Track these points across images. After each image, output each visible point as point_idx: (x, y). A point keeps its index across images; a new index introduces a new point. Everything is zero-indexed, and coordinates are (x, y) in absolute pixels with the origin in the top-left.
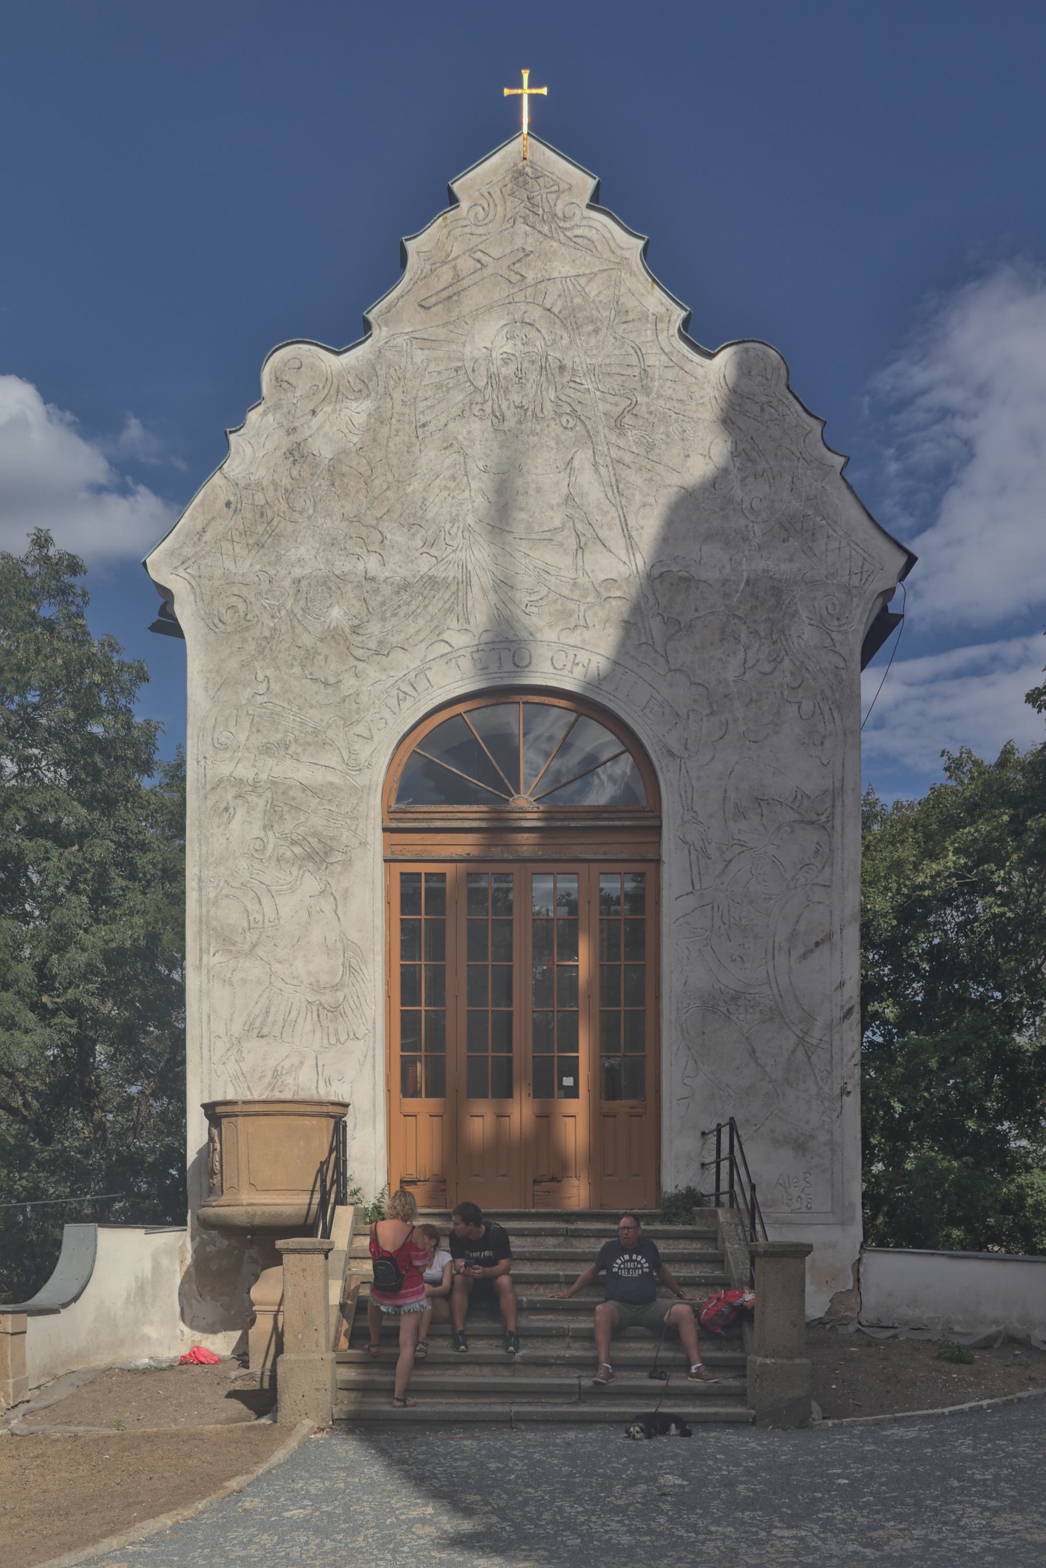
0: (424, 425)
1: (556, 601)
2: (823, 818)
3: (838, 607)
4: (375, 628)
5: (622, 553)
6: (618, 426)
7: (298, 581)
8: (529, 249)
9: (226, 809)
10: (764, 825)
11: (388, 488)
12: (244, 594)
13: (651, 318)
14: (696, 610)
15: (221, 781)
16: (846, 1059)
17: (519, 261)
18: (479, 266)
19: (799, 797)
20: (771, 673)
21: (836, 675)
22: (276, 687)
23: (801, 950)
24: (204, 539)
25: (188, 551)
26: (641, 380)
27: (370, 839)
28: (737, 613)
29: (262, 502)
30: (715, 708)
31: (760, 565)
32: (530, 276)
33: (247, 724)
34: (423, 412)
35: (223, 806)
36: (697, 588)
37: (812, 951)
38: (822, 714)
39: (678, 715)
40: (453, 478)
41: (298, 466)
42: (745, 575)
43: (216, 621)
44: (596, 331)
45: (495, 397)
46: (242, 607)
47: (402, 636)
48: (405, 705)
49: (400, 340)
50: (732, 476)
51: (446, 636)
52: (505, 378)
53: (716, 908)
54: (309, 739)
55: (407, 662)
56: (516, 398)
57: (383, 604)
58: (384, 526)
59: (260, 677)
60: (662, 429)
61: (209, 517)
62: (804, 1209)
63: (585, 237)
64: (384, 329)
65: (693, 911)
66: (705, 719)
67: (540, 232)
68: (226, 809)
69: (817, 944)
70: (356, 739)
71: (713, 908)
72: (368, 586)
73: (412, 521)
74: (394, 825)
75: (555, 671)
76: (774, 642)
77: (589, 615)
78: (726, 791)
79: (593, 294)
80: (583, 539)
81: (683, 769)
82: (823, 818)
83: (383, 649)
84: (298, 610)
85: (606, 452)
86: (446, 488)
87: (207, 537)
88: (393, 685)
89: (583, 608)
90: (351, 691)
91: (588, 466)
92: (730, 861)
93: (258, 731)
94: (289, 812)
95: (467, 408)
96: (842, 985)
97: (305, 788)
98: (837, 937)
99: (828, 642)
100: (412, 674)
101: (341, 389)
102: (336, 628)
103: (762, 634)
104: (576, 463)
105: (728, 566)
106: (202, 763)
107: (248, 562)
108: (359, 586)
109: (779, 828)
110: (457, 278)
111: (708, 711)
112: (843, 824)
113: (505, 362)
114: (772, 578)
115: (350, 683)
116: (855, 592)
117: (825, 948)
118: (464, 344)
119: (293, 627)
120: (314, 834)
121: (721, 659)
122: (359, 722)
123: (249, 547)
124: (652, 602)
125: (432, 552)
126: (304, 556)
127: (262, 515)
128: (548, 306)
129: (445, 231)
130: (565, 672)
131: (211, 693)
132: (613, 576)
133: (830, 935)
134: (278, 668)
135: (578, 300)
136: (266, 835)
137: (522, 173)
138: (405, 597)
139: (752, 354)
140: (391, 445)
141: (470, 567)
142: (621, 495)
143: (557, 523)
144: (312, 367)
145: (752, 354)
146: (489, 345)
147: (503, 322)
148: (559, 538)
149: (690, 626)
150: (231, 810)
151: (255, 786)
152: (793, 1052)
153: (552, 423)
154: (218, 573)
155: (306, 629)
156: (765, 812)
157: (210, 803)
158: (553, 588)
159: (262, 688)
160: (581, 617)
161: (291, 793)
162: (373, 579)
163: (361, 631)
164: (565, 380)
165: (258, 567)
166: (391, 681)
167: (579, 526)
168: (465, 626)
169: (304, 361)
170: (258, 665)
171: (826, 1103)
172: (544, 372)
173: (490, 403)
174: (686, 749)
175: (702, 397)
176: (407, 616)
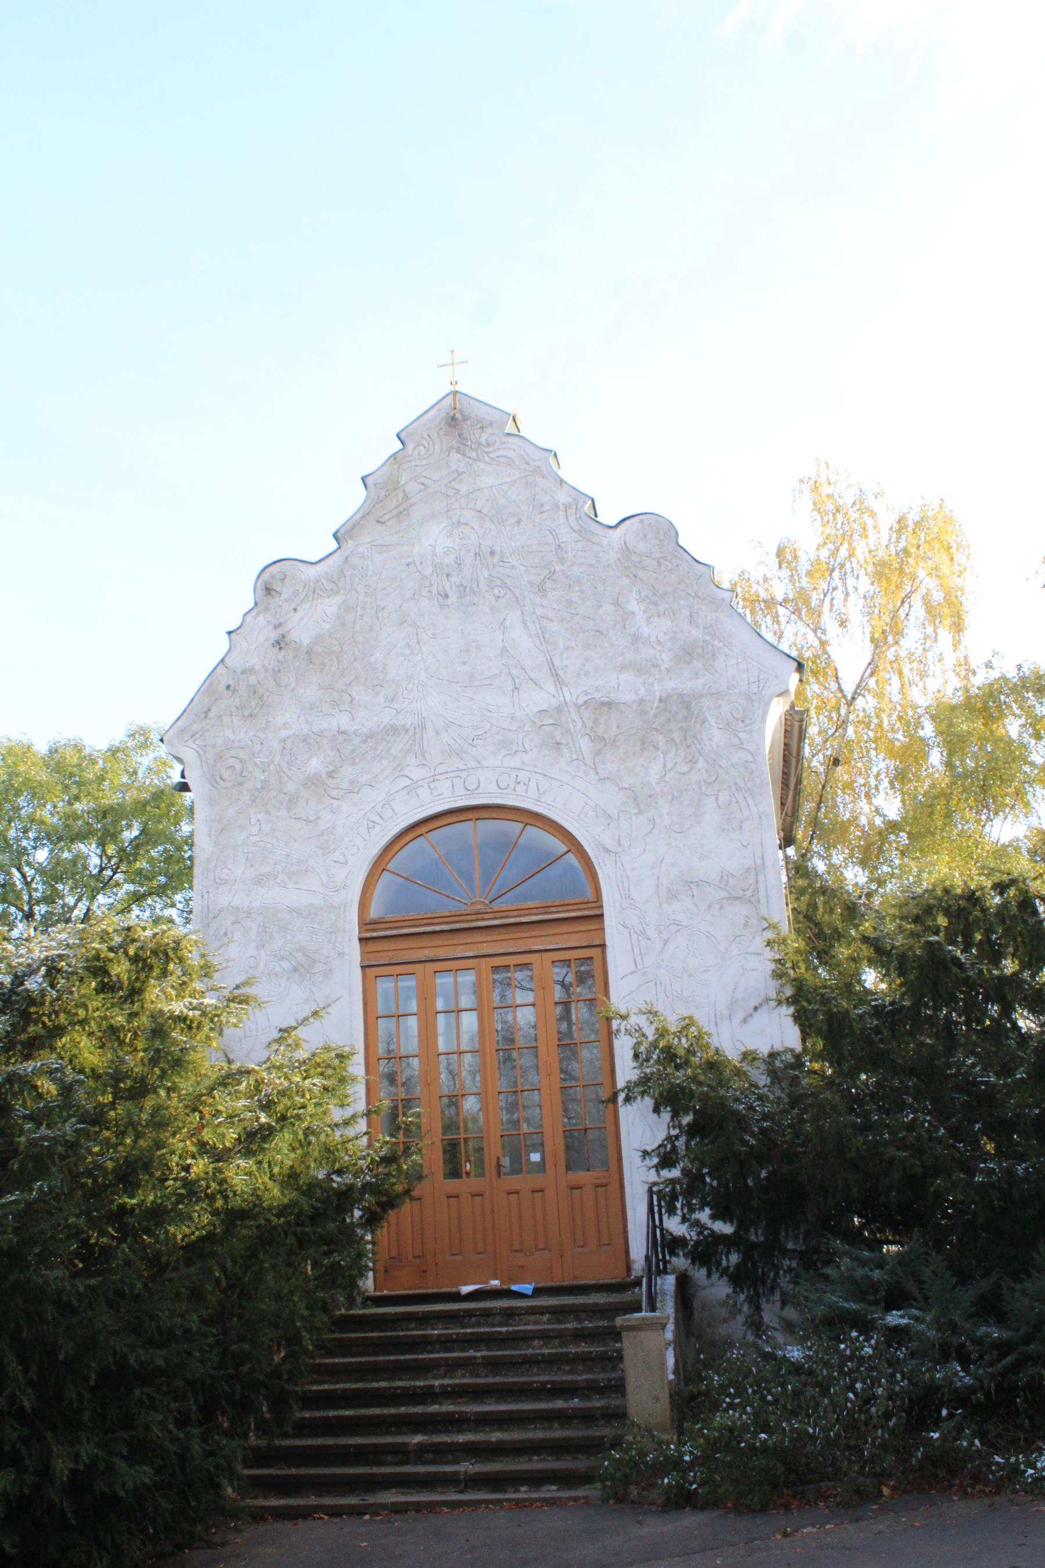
0: (383, 609)
1: (498, 733)
2: (749, 893)
5: (551, 688)
6: (541, 589)
9: (225, 934)
10: (695, 904)
12: (241, 754)
13: (562, 507)
14: (618, 727)
15: (221, 911)
17: (455, 479)
18: (422, 487)
19: (725, 877)
21: (746, 768)
22: (266, 828)
23: (740, 1015)
25: (196, 727)
26: (557, 554)
30: (642, 807)
31: (669, 685)
32: (464, 489)
34: (382, 599)
35: (222, 932)
36: (618, 710)
39: (609, 816)
41: (283, 651)
42: (658, 694)
44: (519, 522)
48: (373, 833)
49: (362, 549)
51: (406, 772)
52: (447, 565)
57: (353, 751)
58: (355, 691)
59: (253, 821)
60: (577, 588)
63: (505, 456)
64: (350, 542)
65: (638, 988)
66: (634, 817)
68: (225, 934)
69: (756, 1009)
72: (341, 738)
73: (375, 683)
74: (368, 935)
76: (689, 747)
78: (658, 879)
80: (517, 681)
81: (619, 863)
83: (353, 788)
84: (283, 764)
86: (403, 655)
87: (211, 715)
89: (521, 736)
93: (252, 866)
97: (292, 910)
99: (736, 741)
100: (380, 806)
101: (317, 590)
102: (314, 775)
103: (678, 741)
104: (508, 623)
105: (642, 689)
106: (206, 897)
107: (244, 730)
108: (334, 739)
109: (710, 906)
112: (767, 897)
115: (327, 818)
116: (754, 697)
117: (763, 1011)
119: (280, 777)
120: (299, 950)
121: (643, 766)
122: (335, 850)
124: (579, 725)
126: (288, 718)
127: (255, 692)
129: (396, 467)
130: (509, 791)
131: (213, 838)
132: (545, 707)
134: (267, 812)
135: (503, 501)
137: (454, 418)
138: (371, 743)
139: (646, 523)
140: (357, 627)
141: (424, 715)
142: (547, 643)
143: (495, 671)
145: (646, 523)
146: (433, 543)
149: (614, 741)
150: (229, 935)
153: (487, 595)
154: (220, 741)
155: (290, 778)
156: (695, 891)
157: (212, 930)
159: (255, 830)
161: (280, 915)
162: (344, 732)
163: (335, 775)
165: (251, 733)
167: (514, 671)
168: (423, 762)
170: (251, 811)
173: (435, 586)
174: (620, 845)
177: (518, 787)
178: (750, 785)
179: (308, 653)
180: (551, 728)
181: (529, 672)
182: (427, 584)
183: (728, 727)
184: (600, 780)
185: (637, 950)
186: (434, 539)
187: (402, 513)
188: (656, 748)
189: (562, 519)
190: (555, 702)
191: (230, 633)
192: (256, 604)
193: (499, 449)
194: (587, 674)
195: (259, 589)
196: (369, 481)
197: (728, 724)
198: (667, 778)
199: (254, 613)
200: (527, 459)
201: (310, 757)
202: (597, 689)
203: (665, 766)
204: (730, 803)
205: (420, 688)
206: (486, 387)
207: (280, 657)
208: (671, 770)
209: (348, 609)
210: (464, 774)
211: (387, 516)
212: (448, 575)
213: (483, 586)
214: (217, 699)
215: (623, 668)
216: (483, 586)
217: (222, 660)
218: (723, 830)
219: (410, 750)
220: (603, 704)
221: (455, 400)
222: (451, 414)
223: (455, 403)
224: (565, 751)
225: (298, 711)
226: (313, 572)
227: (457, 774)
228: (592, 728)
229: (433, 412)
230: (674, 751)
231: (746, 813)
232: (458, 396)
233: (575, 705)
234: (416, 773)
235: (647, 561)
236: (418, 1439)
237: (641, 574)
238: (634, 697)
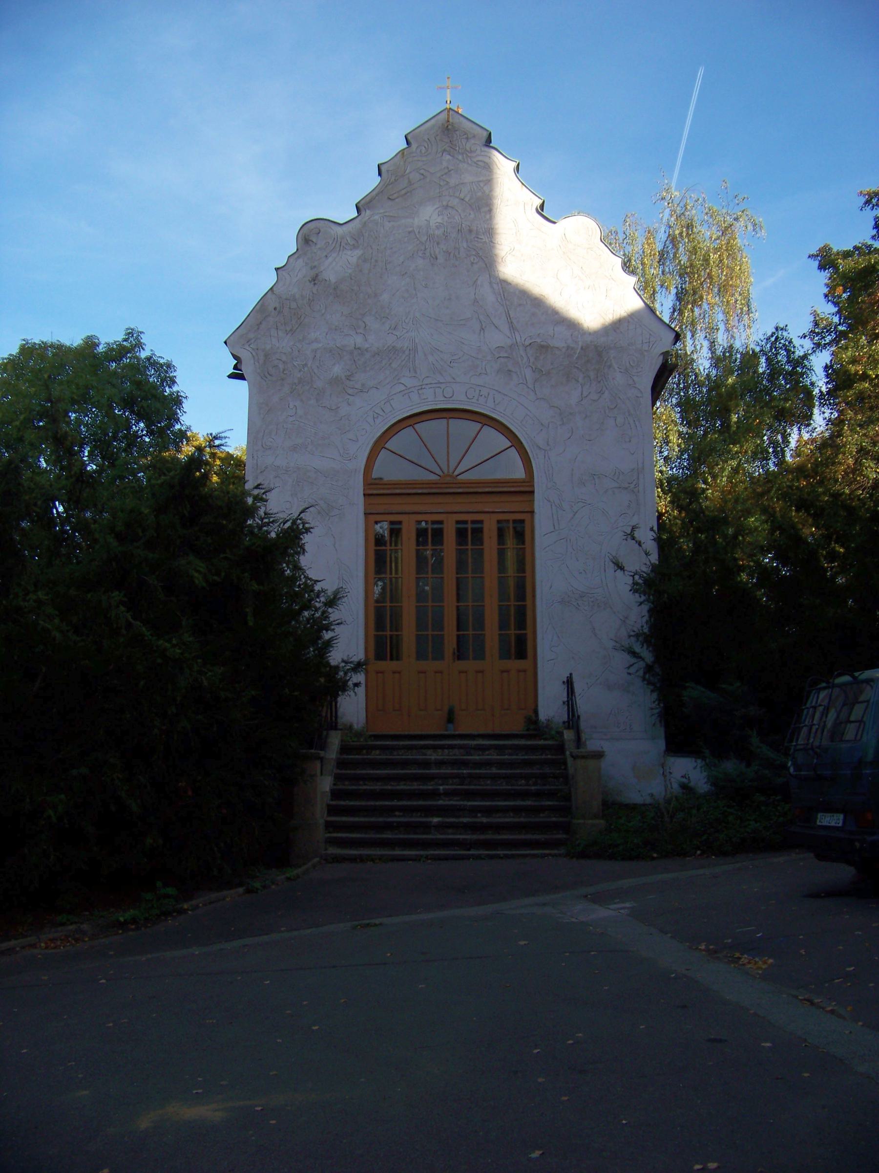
2: (632, 486)
7: (315, 351)
12: (284, 358)
15: (266, 467)
25: (251, 336)
42: (580, 343)
46: (281, 366)
49: (376, 217)
59: (291, 406)
74: (371, 492)
82: (632, 486)
100: (383, 403)
103: (592, 378)
104: (479, 282)
110: (410, 183)
113: (438, 228)
116: (646, 353)
118: (414, 218)
124: (525, 359)
125: (394, 332)
128: (462, 196)
130: (473, 401)
134: (302, 400)
135: (479, 194)
147: (436, 206)
162: (359, 348)
167: (481, 317)
169: (322, 230)
179: (335, 289)
182: (423, 248)
195: (300, 240)
196: (383, 169)
199: (296, 256)
201: (334, 364)
209: (365, 261)
210: (443, 386)
211: (395, 196)
212: (438, 244)
214: (266, 316)
217: (271, 289)
220: (542, 347)
226: (340, 231)
228: (533, 363)
229: (433, 121)
232: (451, 112)
236: (436, 820)
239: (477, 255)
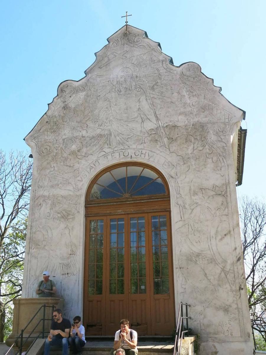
1: (136, 137)
2: (223, 193)
3: (222, 129)
4: (84, 150)
6: (153, 88)
8: (127, 50)
9: (40, 205)
10: (203, 197)
11: (89, 113)
12: (50, 144)
13: (161, 61)
14: (178, 134)
15: (39, 197)
16: (240, 276)
17: (125, 53)
18: (115, 56)
19: (215, 187)
20: (202, 150)
21: (223, 148)
22: (56, 169)
23: (220, 237)
24: (40, 132)
25: (36, 135)
27: (80, 211)
28: (190, 134)
29: (56, 120)
30: (185, 162)
31: (196, 120)
32: (128, 56)
33: (48, 180)
36: (178, 128)
37: (224, 237)
38: (220, 160)
39: (174, 165)
40: (107, 108)
41: (65, 111)
43: (42, 152)
44: (146, 66)
45: (119, 86)
46: (48, 148)
47: (92, 151)
48: (92, 170)
50: (186, 97)
51: (104, 150)
53: (189, 224)
54: (65, 182)
55: (94, 158)
56: (124, 86)
57: (87, 143)
58: (88, 123)
60: (165, 88)
61: (42, 126)
62: (230, 335)
66: (182, 165)
67: (130, 46)
68: (40, 205)
69: (225, 235)
70: (78, 181)
71: (188, 225)
72: (83, 139)
75: (136, 156)
76: (203, 141)
77: (146, 140)
78: (190, 187)
79: (145, 58)
80: (143, 119)
81: (176, 181)
83: (86, 156)
84: (64, 148)
85: (149, 96)
86: (105, 111)
87: (41, 131)
88: (89, 165)
89: (144, 138)
90: (77, 168)
91: (144, 100)
92: (193, 209)
93: (51, 181)
94: (58, 204)
95: (111, 90)
96: (236, 249)
97: (62, 197)
98: (232, 232)
99: (220, 139)
101: (78, 90)
103: (198, 139)
104: (141, 100)
107: (51, 136)
111: (183, 163)
112: (230, 194)
113: (121, 78)
114: (200, 123)
117: (228, 236)
118: (110, 75)
121: (186, 148)
123: (52, 133)
124: (164, 134)
125: (101, 128)
126: (66, 132)
129: (106, 50)
130: (139, 156)
133: (230, 232)
134: (57, 163)
136: (51, 211)
137: (126, 34)
140: (90, 102)
141: (111, 130)
143: (136, 116)
144: (71, 86)
147: (121, 68)
148: (137, 120)
149: (176, 139)
150: (42, 205)
151: (49, 197)
152: (220, 274)
153: (134, 91)
154: (43, 140)
156: (204, 192)
157: (36, 203)
158: (135, 133)
159: (52, 169)
160: (143, 141)
162: (84, 137)
164: (138, 80)
166: (88, 164)
167: (142, 116)
170: (52, 163)
171: (234, 293)
172: (132, 78)
174: (177, 175)
175: (176, 78)
176: (93, 146)
177: (142, 155)
178: (224, 154)
180: (154, 135)
181: (147, 116)
182: (114, 87)
183: (217, 134)
184: (171, 152)
185: (182, 213)
186: (117, 72)
187: (108, 64)
188: (191, 141)
189: (161, 65)
190: (156, 126)
191: (48, 104)
192: (58, 95)
193: (141, 43)
194: (168, 116)
197: (217, 133)
198: (194, 152)
200: (150, 46)
201: (72, 145)
202: (171, 121)
203: (194, 147)
204: (217, 161)
205: (110, 122)
206: (138, 23)
207: (65, 112)
208: (196, 149)
209: (88, 96)
210: (123, 151)
213: (133, 88)
215: (180, 114)
216: (133, 88)
217: (46, 113)
218: (215, 170)
219: (106, 142)
220: (173, 126)
221: (127, 28)
222: (125, 32)
223: (127, 29)
224: (159, 143)
225: (69, 130)
226: (77, 84)
227: (121, 151)
230: (197, 142)
231: (223, 164)
233: (163, 127)
234: (107, 150)
235: (190, 78)
237: (188, 83)
238: (183, 124)
239: (140, 87)
